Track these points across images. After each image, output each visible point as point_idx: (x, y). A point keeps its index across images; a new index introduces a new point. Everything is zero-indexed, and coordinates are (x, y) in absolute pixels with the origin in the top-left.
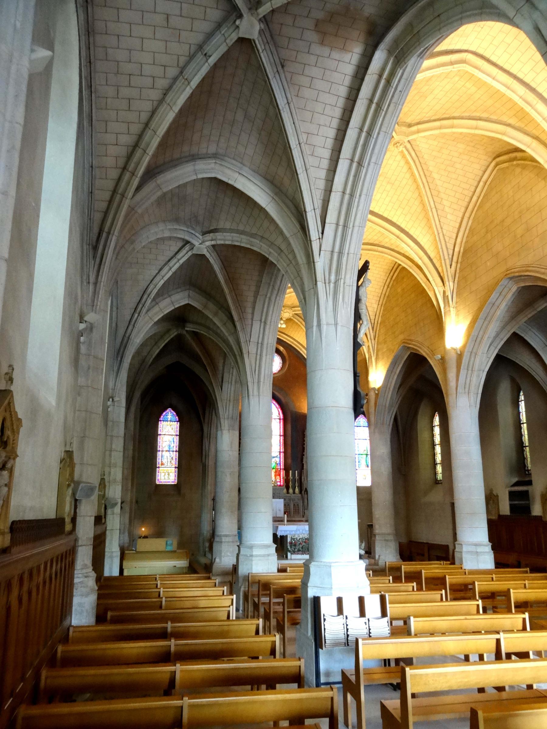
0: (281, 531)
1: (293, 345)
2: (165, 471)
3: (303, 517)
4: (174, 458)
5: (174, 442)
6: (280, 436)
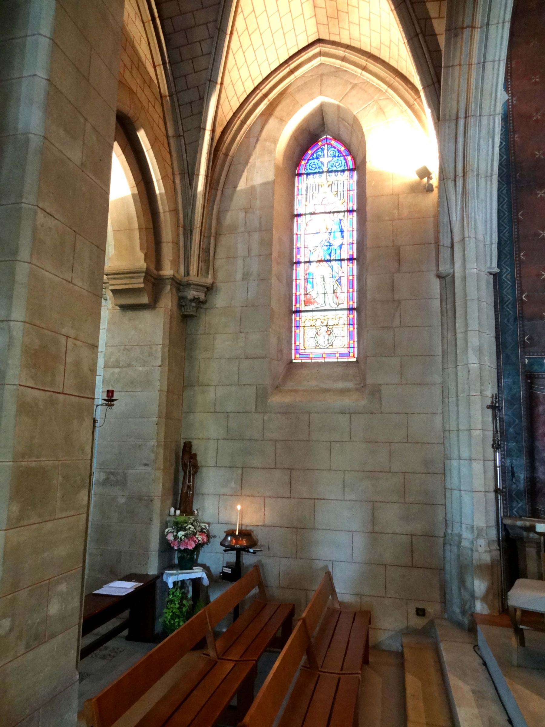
2: (318, 323)
4: (344, 281)
5: (342, 232)
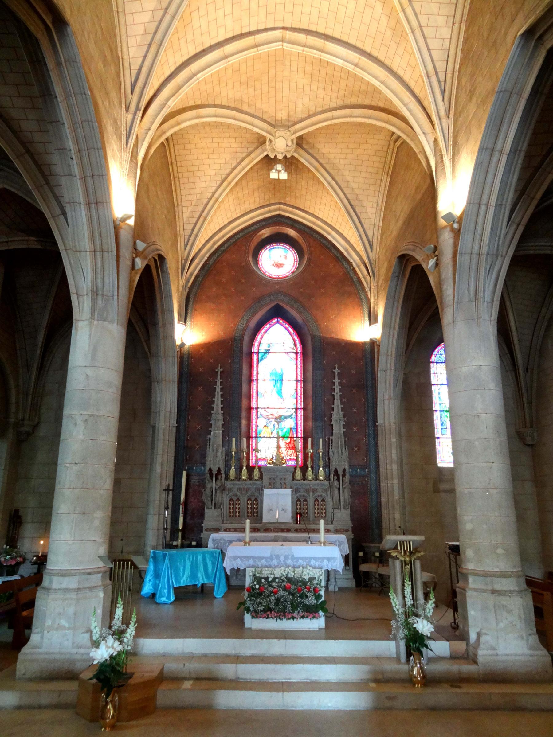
0: (235, 558)
1: (315, 227)
3: (332, 524)
6: (297, 381)
